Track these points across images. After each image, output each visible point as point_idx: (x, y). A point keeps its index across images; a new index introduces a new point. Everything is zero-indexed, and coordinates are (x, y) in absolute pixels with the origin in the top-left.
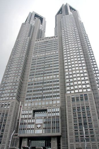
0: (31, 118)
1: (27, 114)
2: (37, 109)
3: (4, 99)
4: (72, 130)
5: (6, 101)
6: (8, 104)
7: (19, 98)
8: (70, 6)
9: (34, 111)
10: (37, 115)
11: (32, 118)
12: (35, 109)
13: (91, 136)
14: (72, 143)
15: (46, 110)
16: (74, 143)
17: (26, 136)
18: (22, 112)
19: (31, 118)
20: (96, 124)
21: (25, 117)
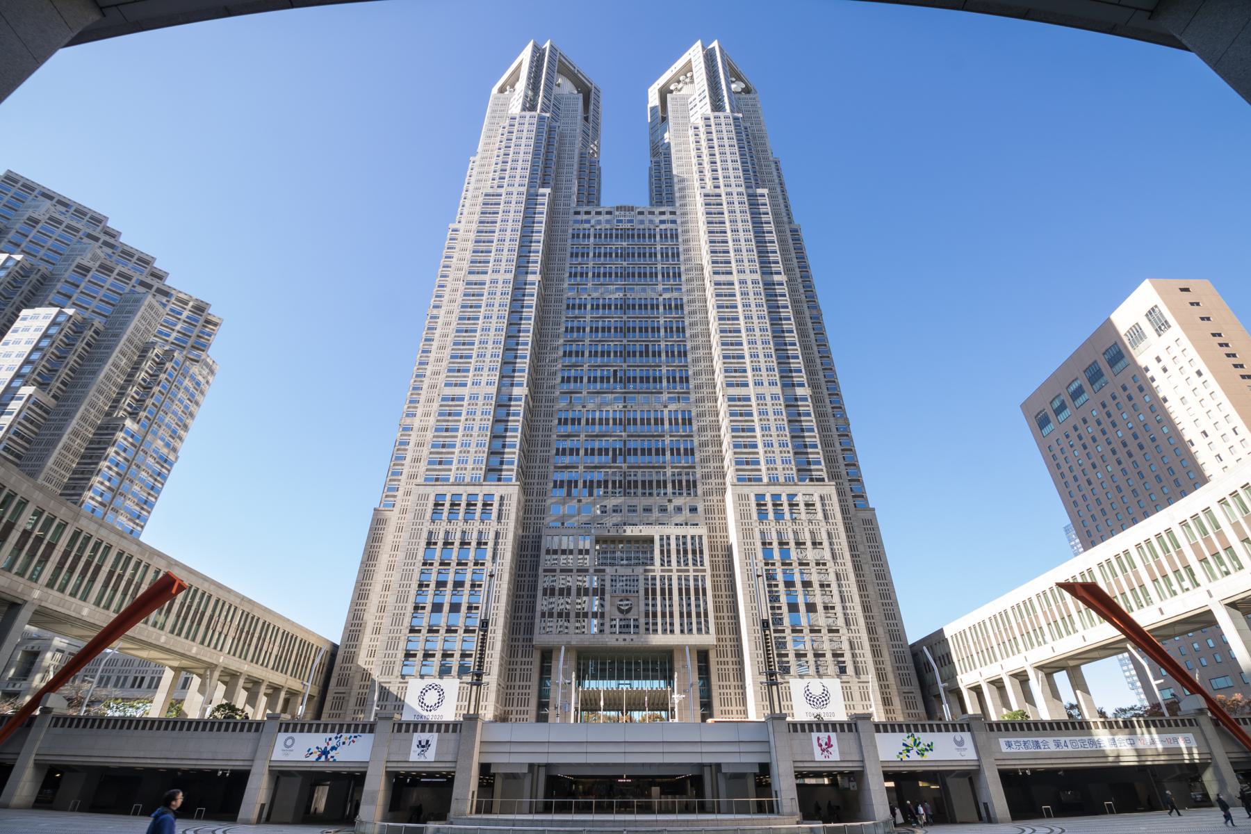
1: (571, 552)
18: (548, 542)
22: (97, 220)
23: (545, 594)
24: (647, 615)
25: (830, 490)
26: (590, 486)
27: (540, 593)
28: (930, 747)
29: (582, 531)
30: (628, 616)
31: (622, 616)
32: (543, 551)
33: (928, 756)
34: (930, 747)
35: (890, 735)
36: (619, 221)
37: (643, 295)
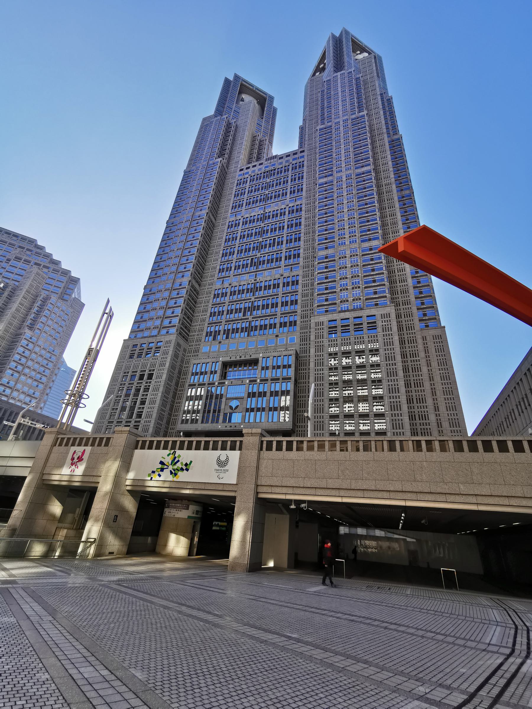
0: (216, 384)
2: (233, 359)
3: (146, 334)
5: (150, 340)
6: (156, 348)
7: (185, 331)
8: (353, 41)
9: (226, 365)
10: (233, 374)
11: (219, 383)
12: (227, 359)
15: (255, 362)
17: (200, 429)
19: (214, 384)
21: (201, 380)
22: (32, 241)
25: (391, 310)
26: (227, 333)
28: (187, 467)
33: (182, 476)
34: (187, 467)
35: (153, 452)
36: (267, 167)
37: (276, 208)
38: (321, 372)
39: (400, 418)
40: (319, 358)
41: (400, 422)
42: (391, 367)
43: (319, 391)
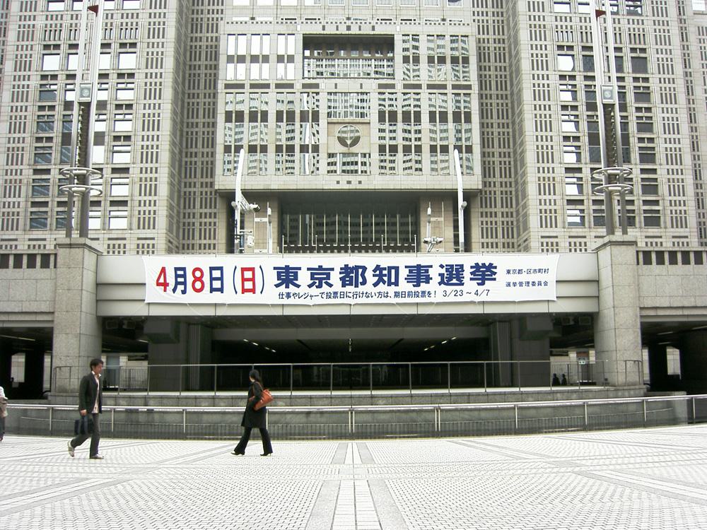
1: (266, 59)
2: (331, 30)
4: (551, 165)
12: (315, 29)
13: (645, 202)
14: (549, 229)
15: (383, 44)
16: (560, 229)
17: (273, 187)
20: (672, 146)
23: (228, 119)
24: (382, 149)
27: (221, 118)
29: (283, 29)
30: (354, 150)
31: (345, 150)
32: (223, 59)
38: (546, 82)
39: (680, 177)
40: (539, 52)
41: (681, 184)
42: (667, 85)
43: (543, 119)
